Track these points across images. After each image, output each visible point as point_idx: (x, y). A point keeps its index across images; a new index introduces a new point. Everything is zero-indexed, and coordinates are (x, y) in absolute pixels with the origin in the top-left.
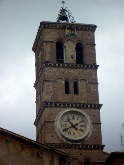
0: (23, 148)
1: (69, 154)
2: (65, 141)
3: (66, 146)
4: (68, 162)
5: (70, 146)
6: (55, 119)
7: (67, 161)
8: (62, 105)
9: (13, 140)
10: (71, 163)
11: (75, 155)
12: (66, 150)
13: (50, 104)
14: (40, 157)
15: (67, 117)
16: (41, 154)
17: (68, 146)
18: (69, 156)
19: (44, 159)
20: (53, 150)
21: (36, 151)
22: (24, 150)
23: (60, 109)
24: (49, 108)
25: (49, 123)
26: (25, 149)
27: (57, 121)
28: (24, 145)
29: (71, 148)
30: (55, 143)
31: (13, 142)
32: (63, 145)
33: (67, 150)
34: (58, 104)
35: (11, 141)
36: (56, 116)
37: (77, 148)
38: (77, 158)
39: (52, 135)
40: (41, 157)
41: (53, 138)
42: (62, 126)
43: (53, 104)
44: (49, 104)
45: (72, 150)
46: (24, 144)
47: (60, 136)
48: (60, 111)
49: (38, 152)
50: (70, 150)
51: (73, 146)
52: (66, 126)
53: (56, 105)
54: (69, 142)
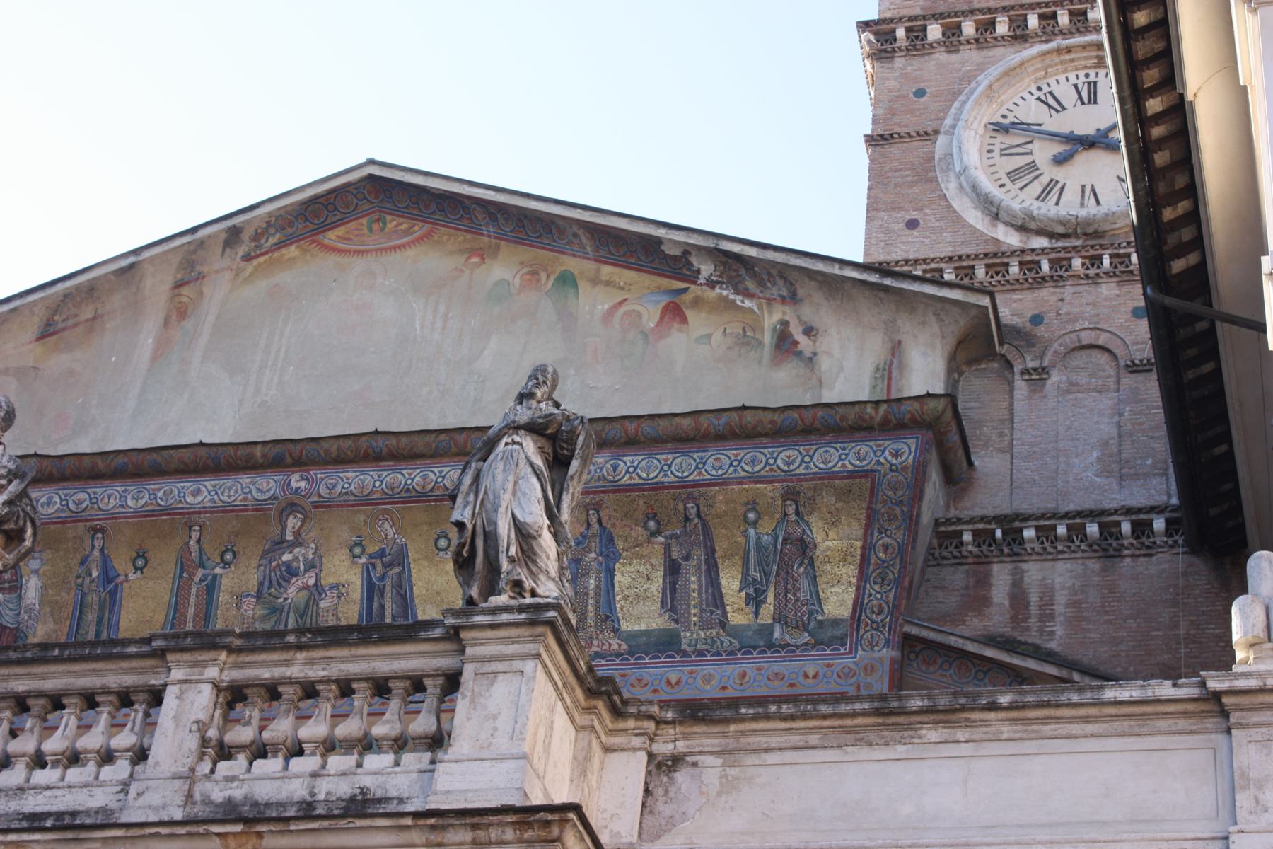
0: (674, 312)
1: (1037, 320)
2: (1013, 239)
3: (1014, 270)
4: (1026, 372)
5: (1045, 266)
6: (944, 118)
7: (1017, 368)
8: (1002, 28)
9: (606, 270)
10: (1055, 377)
11: (1086, 325)
12: (1016, 296)
13: (908, 30)
14: (799, 354)
15: (1037, 94)
16: (809, 331)
17: (1030, 266)
18: (1041, 331)
19: (825, 364)
20: (888, 281)
21: (771, 319)
22: (684, 320)
23: (986, 53)
24: (899, 62)
25: (895, 150)
26: (690, 314)
27: (954, 127)
28: (686, 290)
29: (1056, 280)
30: (924, 260)
31: (608, 283)
32: (987, 266)
33: (1028, 296)
34: (969, 28)
35: (595, 281)
36: (953, 101)
37: (1105, 273)
38: (1102, 339)
39: (915, 215)
40: (807, 354)
41: (915, 233)
42: (996, 154)
43: (934, 32)
44: (901, 33)
45: (1068, 290)
46: (684, 285)
47: (975, 218)
48: (981, 68)
49: (785, 324)
50: (1047, 295)
51: (1077, 263)
52: (1031, 153)
53: (952, 32)
54: (1041, 242)
